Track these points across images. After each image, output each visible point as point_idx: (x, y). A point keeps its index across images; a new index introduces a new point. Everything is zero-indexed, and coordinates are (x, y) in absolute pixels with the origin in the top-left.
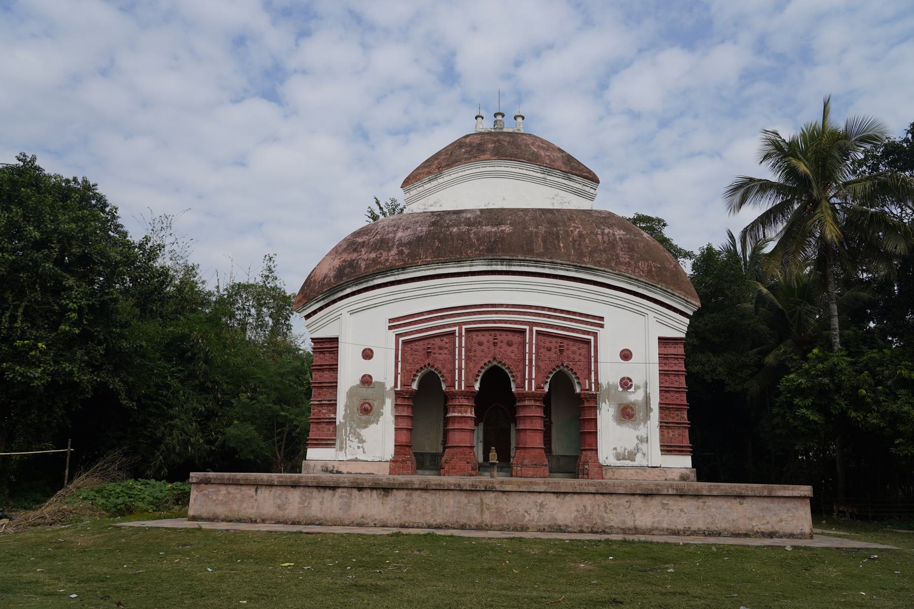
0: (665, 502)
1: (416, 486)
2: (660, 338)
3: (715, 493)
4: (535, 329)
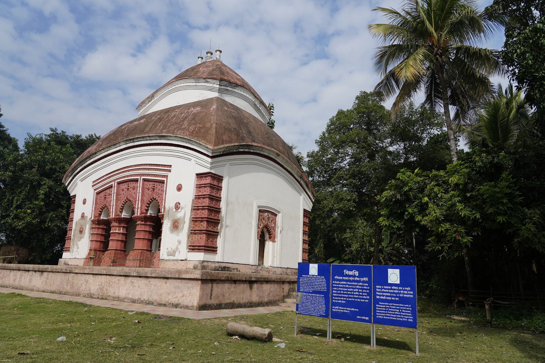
0: (133, 281)
1: (49, 270)
2: (197, 175)
3: (153, 275)
4: (142, 177)
